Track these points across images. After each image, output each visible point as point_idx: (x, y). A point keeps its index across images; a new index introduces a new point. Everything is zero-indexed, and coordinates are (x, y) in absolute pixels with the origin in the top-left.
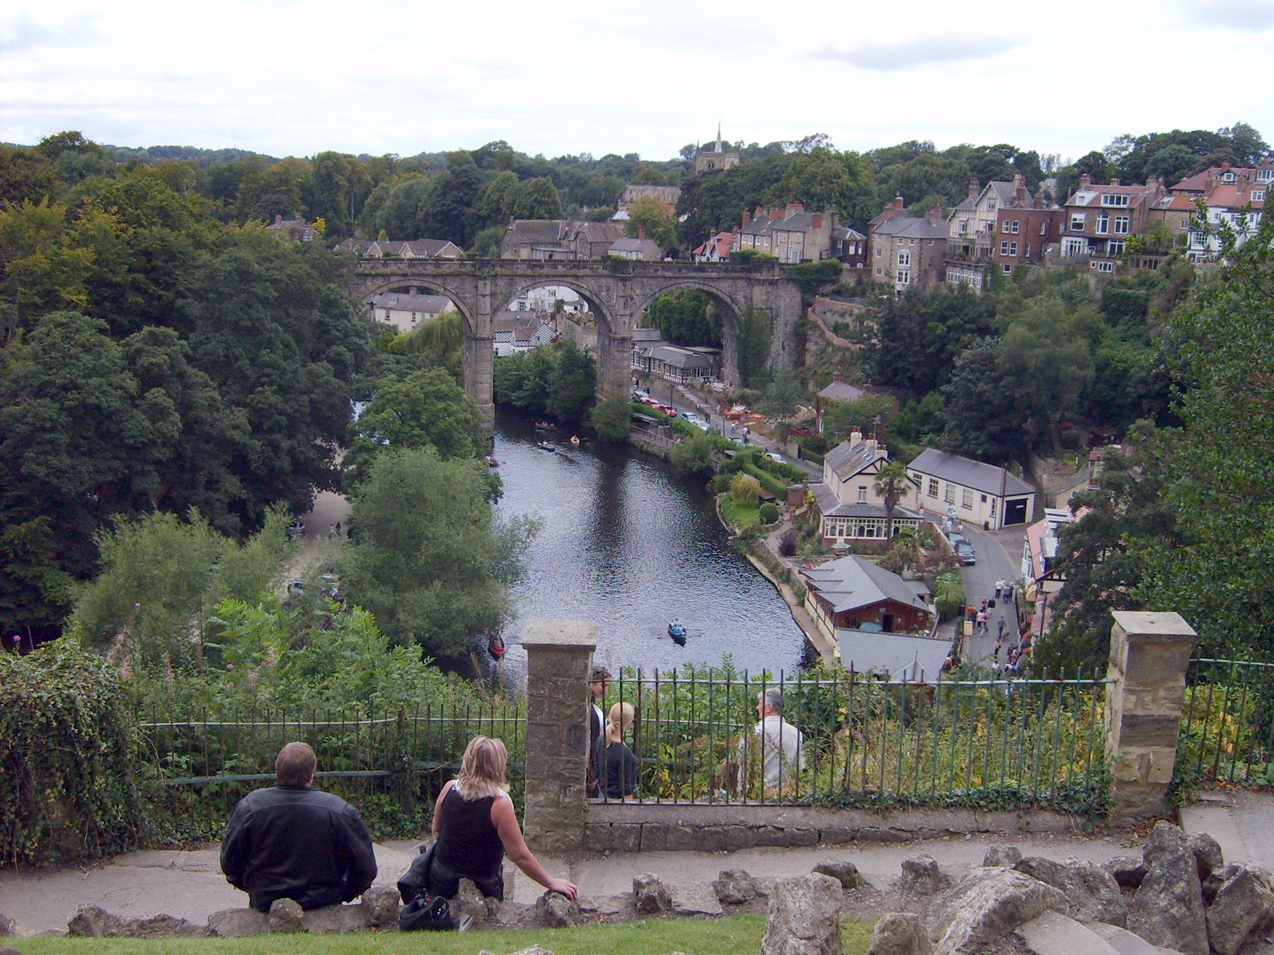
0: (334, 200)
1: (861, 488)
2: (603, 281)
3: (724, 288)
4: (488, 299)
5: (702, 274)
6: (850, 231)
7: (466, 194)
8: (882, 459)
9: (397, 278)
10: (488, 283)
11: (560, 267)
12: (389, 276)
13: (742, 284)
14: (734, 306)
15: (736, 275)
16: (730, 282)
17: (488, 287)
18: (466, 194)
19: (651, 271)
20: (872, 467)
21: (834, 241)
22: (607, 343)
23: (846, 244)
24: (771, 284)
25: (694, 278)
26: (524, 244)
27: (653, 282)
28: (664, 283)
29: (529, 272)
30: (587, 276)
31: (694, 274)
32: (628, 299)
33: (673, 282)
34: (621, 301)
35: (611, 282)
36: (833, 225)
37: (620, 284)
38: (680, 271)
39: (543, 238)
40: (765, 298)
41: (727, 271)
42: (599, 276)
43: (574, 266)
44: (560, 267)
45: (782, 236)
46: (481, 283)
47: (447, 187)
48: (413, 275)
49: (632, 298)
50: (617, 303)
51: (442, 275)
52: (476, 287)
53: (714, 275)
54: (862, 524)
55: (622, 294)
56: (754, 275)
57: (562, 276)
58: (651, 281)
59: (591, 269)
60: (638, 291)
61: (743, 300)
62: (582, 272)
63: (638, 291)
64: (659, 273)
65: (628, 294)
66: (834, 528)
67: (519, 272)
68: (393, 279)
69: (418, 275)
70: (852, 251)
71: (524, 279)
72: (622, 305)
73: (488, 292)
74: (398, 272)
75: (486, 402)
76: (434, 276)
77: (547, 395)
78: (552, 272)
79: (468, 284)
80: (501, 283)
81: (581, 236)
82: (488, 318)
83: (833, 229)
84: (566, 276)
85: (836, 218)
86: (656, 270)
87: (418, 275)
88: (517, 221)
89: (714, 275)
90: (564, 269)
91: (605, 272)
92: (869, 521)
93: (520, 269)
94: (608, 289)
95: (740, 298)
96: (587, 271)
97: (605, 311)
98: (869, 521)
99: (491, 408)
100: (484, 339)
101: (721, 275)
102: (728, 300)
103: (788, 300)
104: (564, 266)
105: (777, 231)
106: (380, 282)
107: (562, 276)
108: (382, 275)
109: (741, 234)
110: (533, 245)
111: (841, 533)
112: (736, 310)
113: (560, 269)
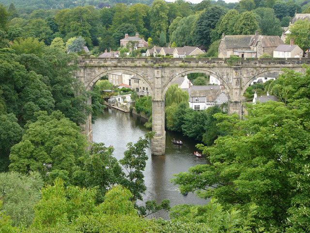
0: (159, 25)
2: (225, 70)
4: (159, 80)
5: (283, 65)
7: (212, 21)
11: (200, 62)
17: (160, 73)
18: (212, 21)
25: (279, 67)
31: (278, 65)
32: (239, 81)
35: (229, 70)
38: (270, 63)
41: (298, 63)
44: (200, 62)
46: (156, 71)
48: (120, 67)
50: (233, 82)
51: (136, 67)
53: (291, 65)
58: (252, 69)
63: (245, 75)
64: (257, 65)
67: (177, 65)
68: (109, 69)
69: (123, 67)
71: (180, 69)
73: (160, 76)
74: (112, 65)
75: (159, 135)
76: (131, 67)
77: (204, 131)
80: (167, 71)
81: (259, 43)
82: (160, 91)
86: (256, 63)
87: (123, 67)
88: (226, 36)
89: (291, 65)
91: (226, 65)
94: (228, 75)
96: (216, 64)
100: (158, 101)
101: (295, 65)
107: (201, 67)
113: (200, 63)
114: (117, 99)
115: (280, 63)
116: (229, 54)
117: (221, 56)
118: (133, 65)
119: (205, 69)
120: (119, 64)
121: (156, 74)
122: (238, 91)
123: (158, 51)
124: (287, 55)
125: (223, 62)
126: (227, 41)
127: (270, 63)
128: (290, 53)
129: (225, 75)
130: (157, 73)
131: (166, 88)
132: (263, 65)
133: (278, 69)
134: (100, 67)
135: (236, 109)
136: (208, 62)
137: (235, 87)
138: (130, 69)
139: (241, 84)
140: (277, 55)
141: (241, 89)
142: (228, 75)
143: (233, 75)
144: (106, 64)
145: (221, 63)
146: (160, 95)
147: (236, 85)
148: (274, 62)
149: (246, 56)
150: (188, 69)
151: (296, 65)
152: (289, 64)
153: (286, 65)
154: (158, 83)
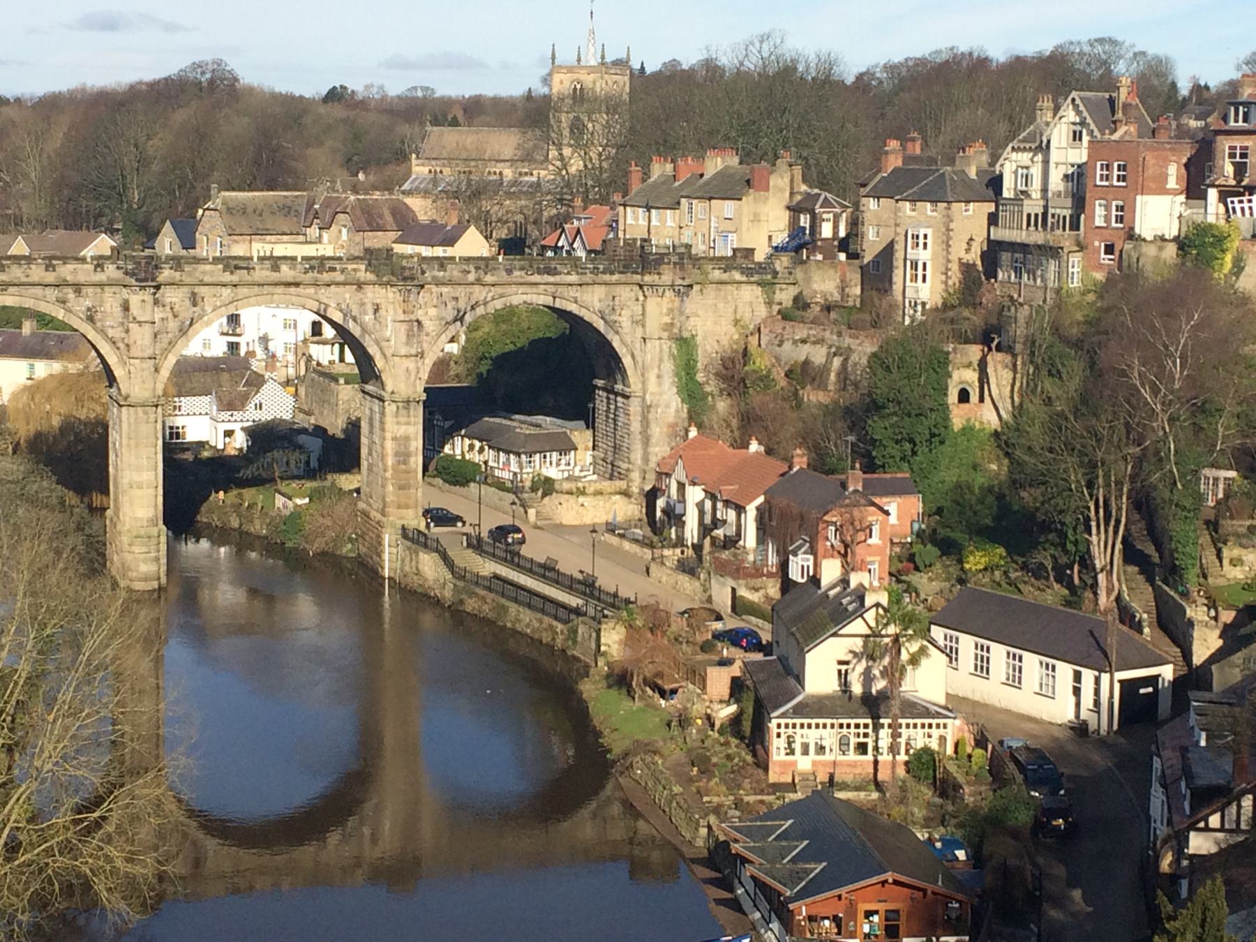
1: (841, 663)
5: (551, 279)
8: (877, 605)
13: (626, 294)
14: (609, 336)
15: (616, 277)
19: (456, 273)
20: (860, 619)
21: (795, 210)
22: (376, 409)
29: (227, 277)
30: (338, 284)
31: (536, 278)
33: (499, 290)
36: (792, 188)
40: (667, 320)
41: (595, 271)
43: (312, 268)
53: (573, 278)
54: (845, 731)
55: (402, 317)
57: (288, 284)
59: (343, 271)
60: (432, 312)
62: (326, 277)
65: (413, 317)
66: (790, 741)
72: (403, 338)
78: (275, 276)
79: (110, 303)
83: (792, 194)
84: (297, 285)
85: (798, 171)
90: (292, 273)
92: (857, 726)
96: (338, 277)
97: (372, 350)
98: (857, 726)
102: (600, 325)
103: (709, 323)
104: (293, 267)
107: (288, 284)
109: (625, 205)
111: (805, 752)
118: (50, 277)
121: (135, 310)
122: (411, 364)
125: (363, 267)
129: (371, 312)
131: (170, 356)
133: (535, 290)
135: (408, 424)
137: (403, 351)
138: (38, 291)
141: (421, 355)
145: (355, 270)
147: (407, 344)
151: (589, 278)
152: (568, 273)
153: (557, 279)
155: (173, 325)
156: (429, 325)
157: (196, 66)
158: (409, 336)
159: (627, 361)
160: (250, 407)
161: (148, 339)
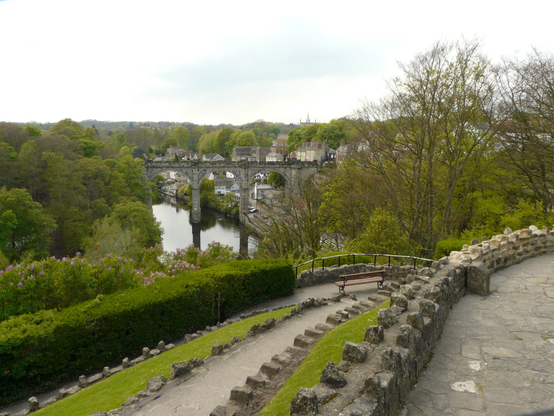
2: (238, 169)
3: (281, 171)
5: (273, 166)
6: (332, 149)
9: (165, 168)
10: (197, 170)
12: (162, 168)
13: (288, 169)
15: (286, 166)
16: (284, 169)
17: (197, 171)
21: (326, 153)
23: (330, 154)
24: (298, 169)
26: (237, 154)
27: (256, 169)
28: (259, 169)
29: (211, 166)
34: (244, 175)
35: (240, 169)
37: (243, 170)
38: (265, 165)
39: (245, 153)
42: (236, 167)
45: (308, 152)
47: (221, 135)
49: (248, 175)
50: (243, 176)
52: (193, 171)
53: (278, 166)
56: (292, 166)
58: (254, 169)
60: (250, 172)
61: (288, 175)
62: (230, 166)
64: (258, 166)
67: (208, 166)
68: (163, 168)
70: (332, 156)
78: (220, 165)
79: (190, 170)
84: (224, 167)
91: (238, 165)
93: (208, 165)
94: (239, 171)
95: (288, 174)
96: (232, 165)
99: (199, 213)
100: (195, 189)
105: (307, 150)
106: (159, 169)
108: (159, 167)
110: (242, 155)
112: (286, 178)
113: (222, 165)
114: (167, 188)
115: (271, 164)
116: (239, 159)
117: (233, 160)
118: (179, 166)
119: (225, 168)
120: (170, 166)
121: (194, 172)
122: (246, 182)
123: (193, 156)
124: (275, 160)
126: (237, 150)
127: (265, 165)
128: (276, 158)
130: (195, 171)
132: (261, 166)
134: (157, 167)
136: (227, 164)
138: (177, 168)
139: (248, 178)
140: (268, 159)
141: (248, 180)
142: (239, 171)
143: (243, 172)
144: (161, 166)
146: (197, 185)
148: (267, 164)
149: (249, 160)
150: (215, 168)
151: (281, 166)
154: (196, 177)
155: (201, 174)
156: (250, 175)
157: (258, 120)
158: (245, 177)
159: (289, 182)
160: (231, 188)
161: (197, 177)
